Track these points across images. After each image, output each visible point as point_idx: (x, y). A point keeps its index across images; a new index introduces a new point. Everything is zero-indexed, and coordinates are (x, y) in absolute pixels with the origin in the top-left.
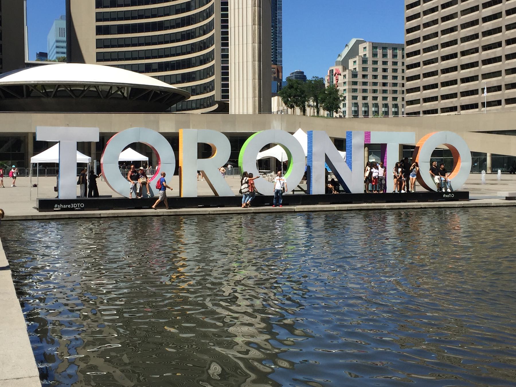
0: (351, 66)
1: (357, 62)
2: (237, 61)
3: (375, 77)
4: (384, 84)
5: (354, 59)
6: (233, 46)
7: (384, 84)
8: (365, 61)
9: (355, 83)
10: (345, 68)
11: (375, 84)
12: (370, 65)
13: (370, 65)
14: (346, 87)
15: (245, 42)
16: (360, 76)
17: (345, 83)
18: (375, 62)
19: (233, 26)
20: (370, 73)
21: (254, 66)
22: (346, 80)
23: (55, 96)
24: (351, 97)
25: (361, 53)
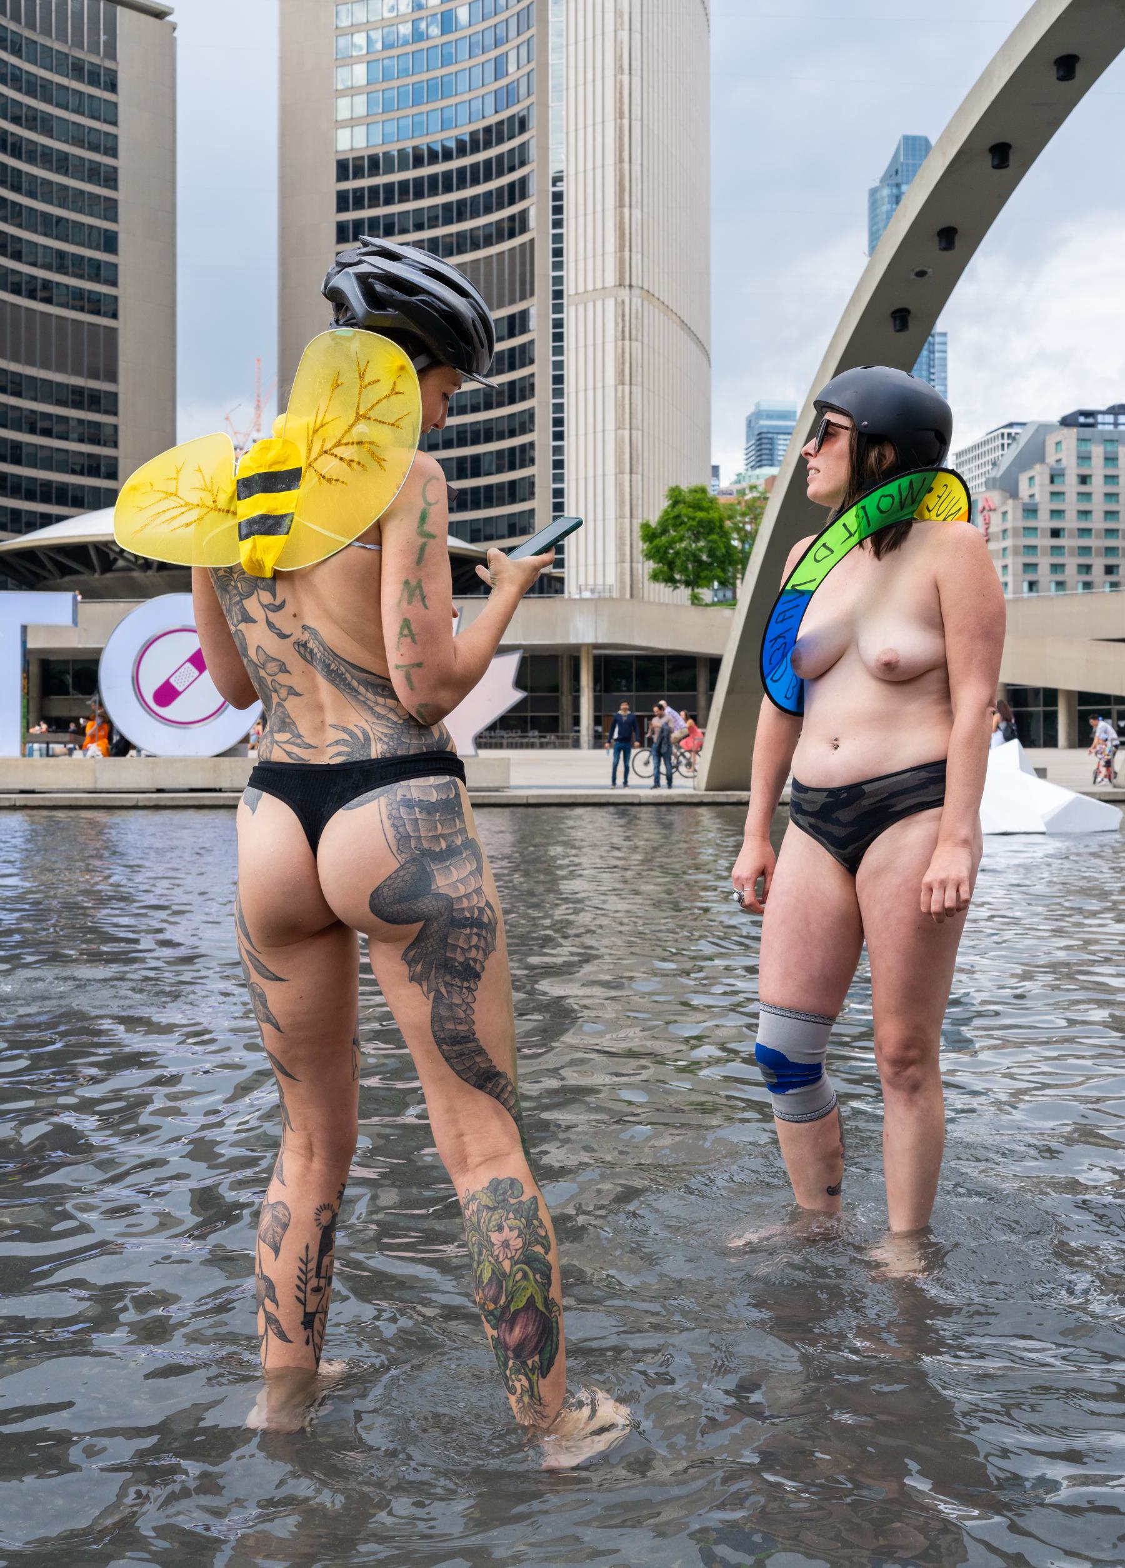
0: (1024, 490)
1: (1037, 480)
2: (582, 475)
3: (1085, 514)
4: (1056, 533)
5: (1030, 473)
6: (573, 439)
7: (1056, 533)
9: (1031, 530)
10: (1014, 494)
11: (1085, 532)
12: (1070, 485)
14: (1009, 543)
15: (599, 428)
17: (1005, 531)
18: (1084, 479)
19: (572, 388)
20: (1071, 504)
21: (619, 486)
22: (1009, 525)
24: (1020, 567)
25: (1051, 459)
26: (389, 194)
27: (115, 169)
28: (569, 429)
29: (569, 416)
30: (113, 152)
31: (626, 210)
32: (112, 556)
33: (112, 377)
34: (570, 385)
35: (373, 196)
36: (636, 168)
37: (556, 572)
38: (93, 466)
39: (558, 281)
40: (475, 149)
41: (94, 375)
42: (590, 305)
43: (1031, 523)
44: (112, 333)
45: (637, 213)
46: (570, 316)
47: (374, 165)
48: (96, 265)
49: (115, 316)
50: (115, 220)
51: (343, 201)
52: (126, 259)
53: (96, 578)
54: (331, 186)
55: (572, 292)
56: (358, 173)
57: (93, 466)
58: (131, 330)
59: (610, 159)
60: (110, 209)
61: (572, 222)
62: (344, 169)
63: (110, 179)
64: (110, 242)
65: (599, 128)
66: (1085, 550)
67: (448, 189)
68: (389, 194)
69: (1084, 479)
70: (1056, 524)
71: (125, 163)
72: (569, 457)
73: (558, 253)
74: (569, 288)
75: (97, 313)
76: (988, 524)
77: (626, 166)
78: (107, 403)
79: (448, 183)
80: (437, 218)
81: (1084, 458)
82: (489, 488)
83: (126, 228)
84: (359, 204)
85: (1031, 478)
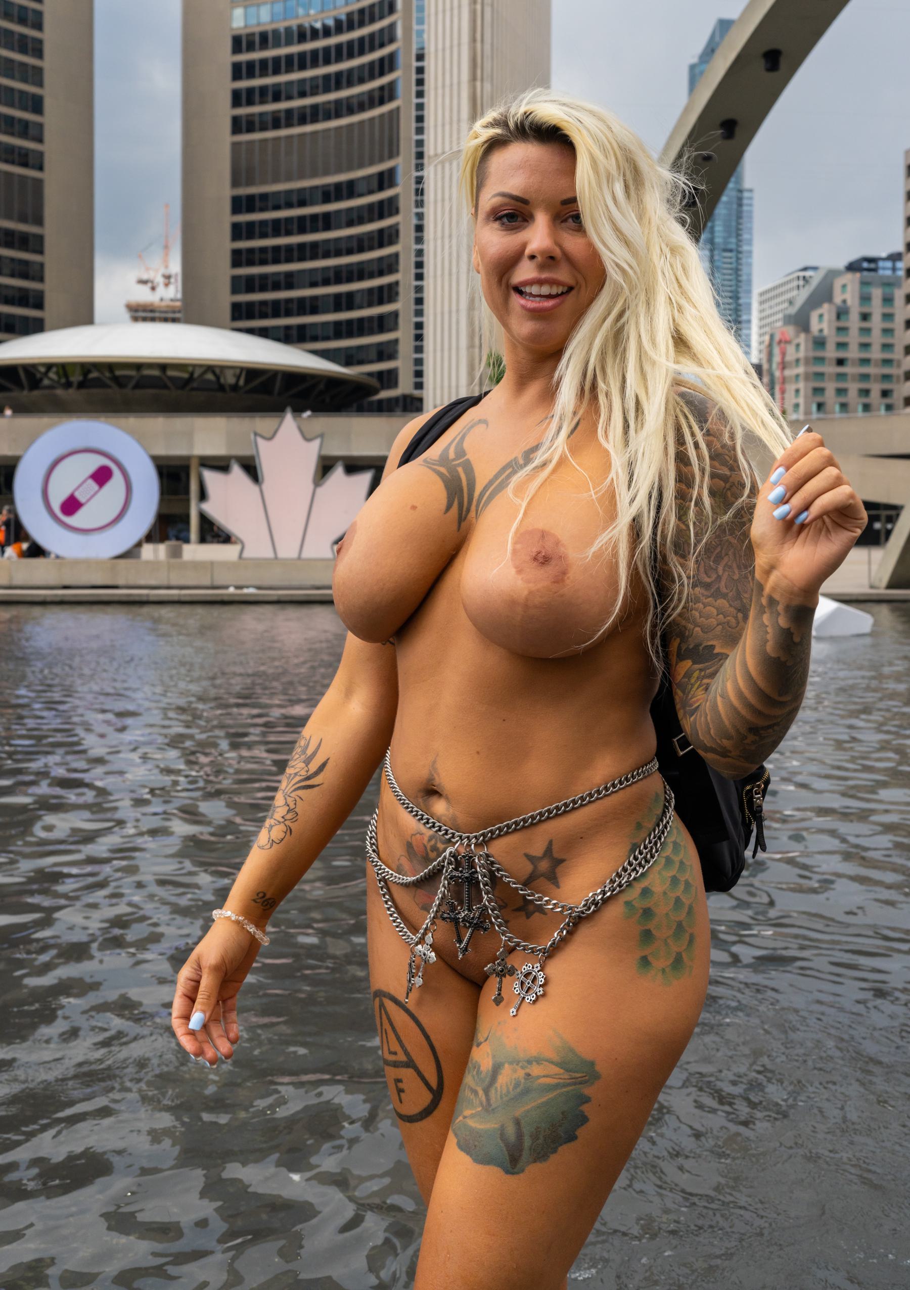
0: (815, 326)
1: (826, 317)
3: (865, 346)
7: (840, 362)
8: (841, 313)
9: (820, 360)
12: (854, 321)
13: (854, 321)
14: (801, 370)
16: (831, 346)
17: (798, 361)
18: (865, 317)
20: (854, 338)
23: (81, 385)
24: (810, 392)
25: (838, 299)
26: (277, 66)
27: (40, 42)
28: (429, 270)
29: (429, 260)
30: (39, 26)
31: (478, 84)
32: (38, 376)
33: (39, 220)
34: (429, 233)
35: (264, 68)
36: (487, 47)
37: (416, 393)
38: (24, 298)
39: (420, 143)
40: (351, 27)
41: (23, 219)
42: (447, 165)
43: (819, 354)
44: (39, 183)
45: (488, 86)
46: (429, 173)
47: (264, 39)
48: (26, 124)
49: (41, 168)
50: (40, 84)
51: (238, 72)
52: (53, 118)
53: (25, 395)
54: (227, 58)
55: (432, 153)
56: (251, 47)
57: (24, 298)
58: (54, 179)
59: (465, 38)
60: (36, 76)
61: (432, 93)
62: (239, 43)
63: (37, 49)
64: (36, 105)
65: (456, 12)
66: (865, 377)
67: (327, 62)
68: (277, 66)
69: (865, 317)
70: (841, 354)
71: (49, 35)
72: (429, 295)
73: (420, 119)
74: (429, 150)
75: (25, 165)
76: (783, 354)
77: (479, 45)
78: (34, 244)
79: (328, 55)
80: (317, 87)
81: (865, 299)
82: (361, 320)
83: (52, 94)
84: (251, 75)
85: (821, 316)
